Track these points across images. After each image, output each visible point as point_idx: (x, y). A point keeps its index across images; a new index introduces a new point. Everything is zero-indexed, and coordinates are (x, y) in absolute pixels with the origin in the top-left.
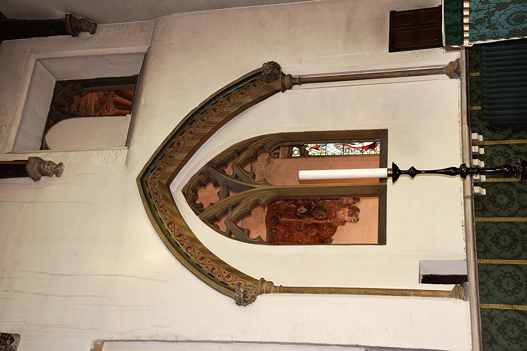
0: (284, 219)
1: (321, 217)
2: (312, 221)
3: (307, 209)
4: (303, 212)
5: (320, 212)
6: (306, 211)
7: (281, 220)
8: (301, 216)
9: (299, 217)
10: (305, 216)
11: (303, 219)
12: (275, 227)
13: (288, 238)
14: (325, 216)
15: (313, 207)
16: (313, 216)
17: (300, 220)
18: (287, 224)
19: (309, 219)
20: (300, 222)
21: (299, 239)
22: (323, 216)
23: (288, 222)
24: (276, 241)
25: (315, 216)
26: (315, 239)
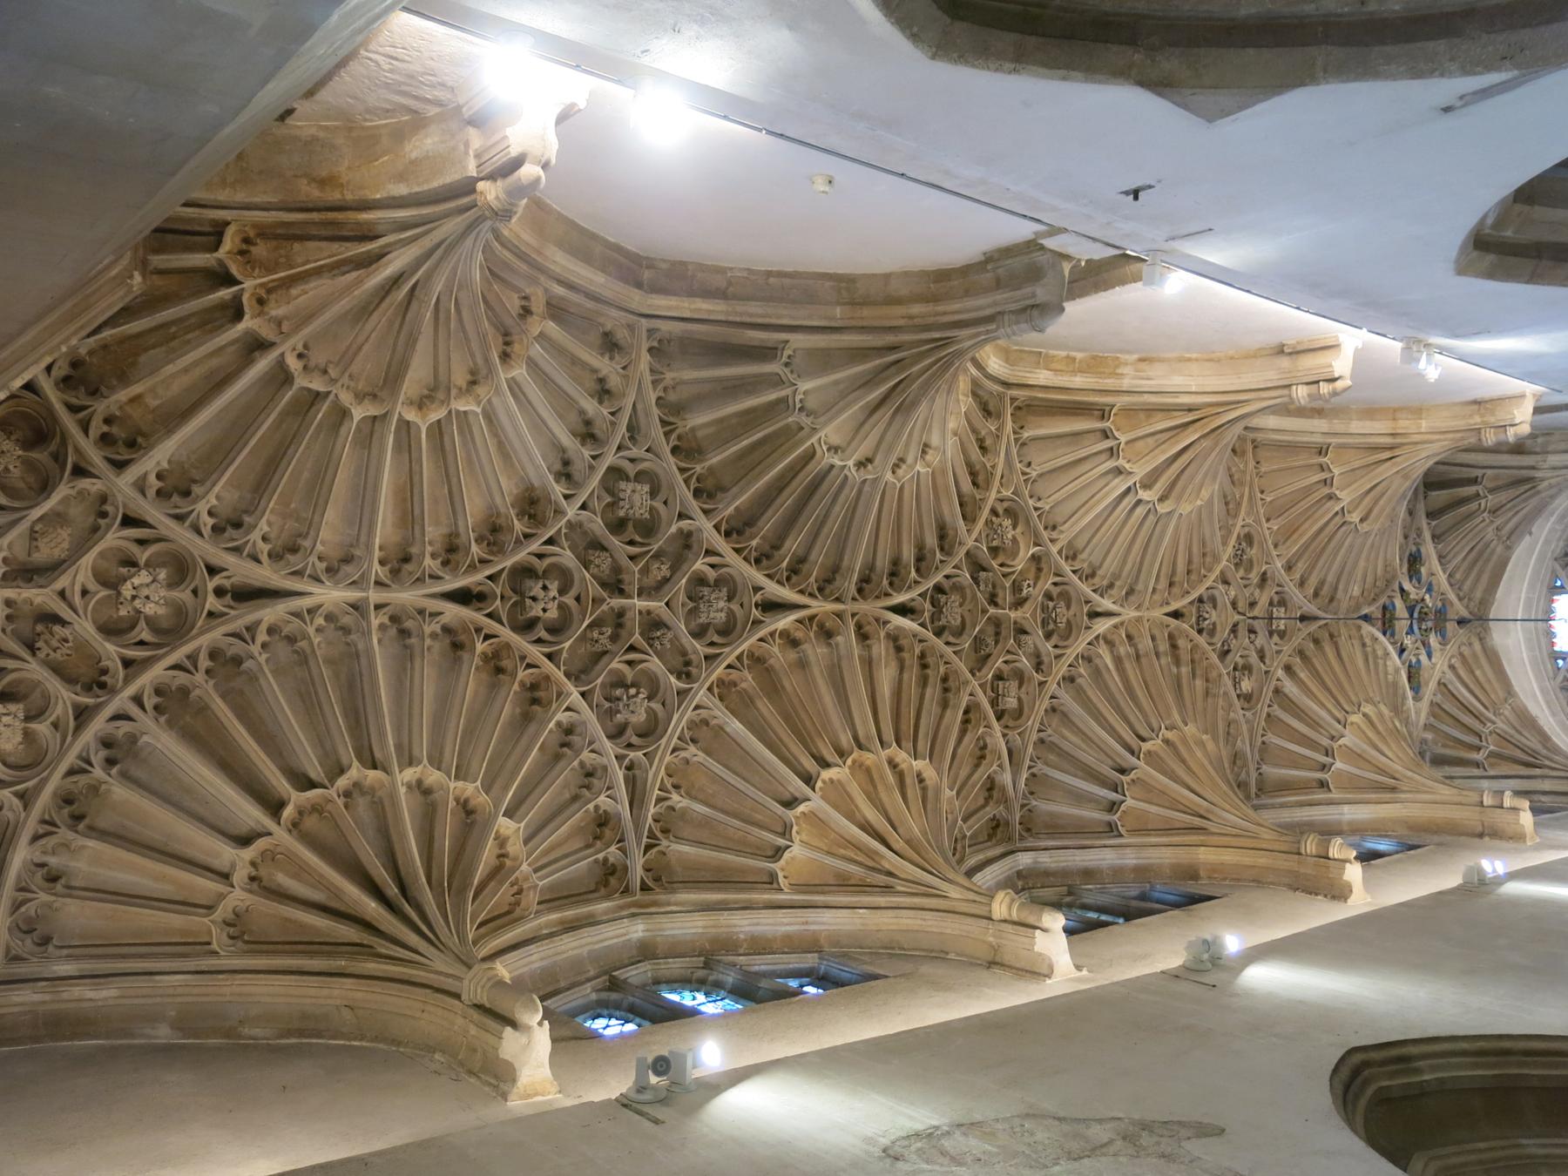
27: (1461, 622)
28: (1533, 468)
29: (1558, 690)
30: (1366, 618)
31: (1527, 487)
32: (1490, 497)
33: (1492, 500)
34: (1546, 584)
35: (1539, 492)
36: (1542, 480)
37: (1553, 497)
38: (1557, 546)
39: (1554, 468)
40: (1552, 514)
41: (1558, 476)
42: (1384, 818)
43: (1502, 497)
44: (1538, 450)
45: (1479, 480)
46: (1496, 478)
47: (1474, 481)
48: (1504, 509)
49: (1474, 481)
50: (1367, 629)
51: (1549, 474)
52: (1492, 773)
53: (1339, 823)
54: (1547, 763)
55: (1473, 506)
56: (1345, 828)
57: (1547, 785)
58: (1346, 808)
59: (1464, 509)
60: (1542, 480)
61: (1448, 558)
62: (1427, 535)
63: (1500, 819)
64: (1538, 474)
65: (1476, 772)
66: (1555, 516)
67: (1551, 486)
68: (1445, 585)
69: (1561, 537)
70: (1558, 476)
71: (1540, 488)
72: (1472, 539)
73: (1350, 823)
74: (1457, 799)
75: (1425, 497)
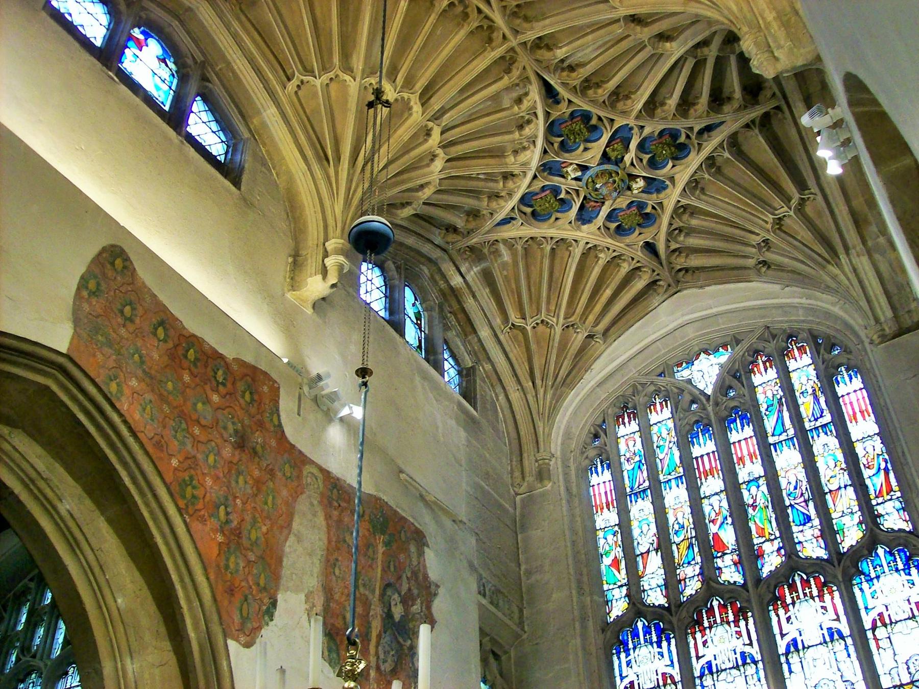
0: (381, 549)
1: (382, 656)
2: (376, 625)
3: (399, 622)
4: (393, 609)
5: (393, 655)
6: (395, 617)
7: (380, 538)
8: (386, 598)
9: (383, 594)
10: (386, 610)
11: (379, 600)
12: (366, 517)
13: (345, 541)
14: (383, 668)
15: (401, 640)
16: (385, 632)
17: (377, 592)
18: (371, 550)
19: (379, 616)
20: (373, 591)
21: (340, 570)
22: (385, 661)
23: (375, 556)
24: (340, 506)
25: (386, 640)
26: (338, 616)
27: (650, 248)
28: (847, 249)
29: (632, 382)
30: (550, 92)
31: (826, 256)
32: (792, 213)
33: (793, 223)
34: (736, 331)
35: (824, 268)
36: (839, 265)
37: (827, 289)
38: (782, 322)
39: (855, 270)
40: (809, 297)
41: (848, 279)
42: (284, 158)
43: (804, 234)
44: (870, 243)
45: (806, 192)
46: (819, 214)
47: (802, 186)
48: (791, 240)
49: (802, 186)
50: (535, 94)
51: (847, 269)
52: (502, 337)
53: (259, 113)
54: (541, 391)
55: (777, 202)
56: (255, 121)
57: (515, 396)
58: (273, 110)
59: (765, 191)
60: (839, 265)
61: (703, 197)
62: (708, 148)
63: (312, 263)
64: (843, 257)
65: (498, 321)
66: (809, 301)
67: (834, 278)
68: (669, 206)
69: (791, 321)
70: (848, 279)
71: (830, 267)
72: (738, 216)
73: (264, 125)
74: (331, 221)
75: (747, 126)
